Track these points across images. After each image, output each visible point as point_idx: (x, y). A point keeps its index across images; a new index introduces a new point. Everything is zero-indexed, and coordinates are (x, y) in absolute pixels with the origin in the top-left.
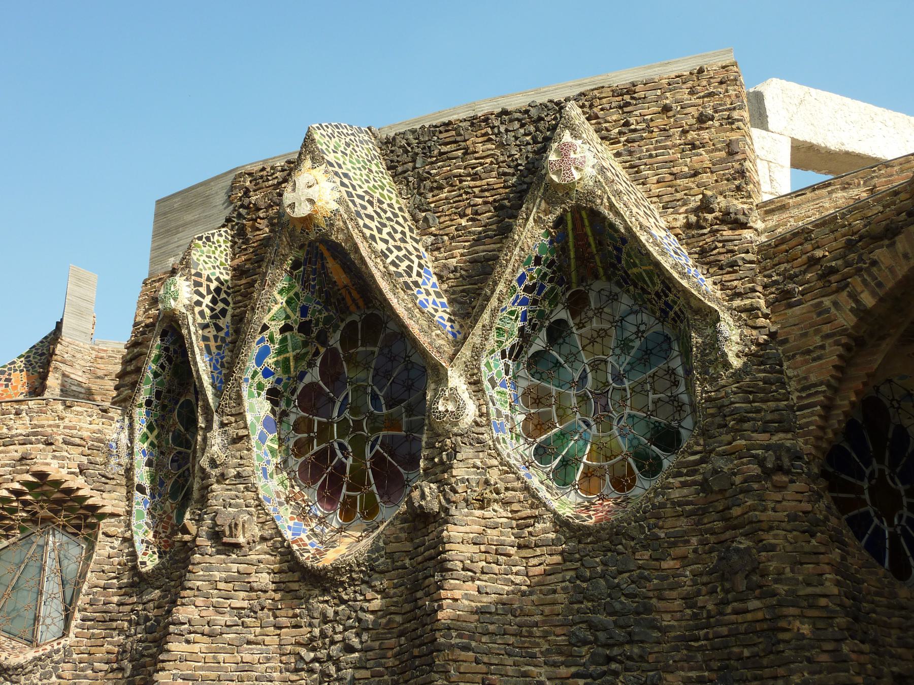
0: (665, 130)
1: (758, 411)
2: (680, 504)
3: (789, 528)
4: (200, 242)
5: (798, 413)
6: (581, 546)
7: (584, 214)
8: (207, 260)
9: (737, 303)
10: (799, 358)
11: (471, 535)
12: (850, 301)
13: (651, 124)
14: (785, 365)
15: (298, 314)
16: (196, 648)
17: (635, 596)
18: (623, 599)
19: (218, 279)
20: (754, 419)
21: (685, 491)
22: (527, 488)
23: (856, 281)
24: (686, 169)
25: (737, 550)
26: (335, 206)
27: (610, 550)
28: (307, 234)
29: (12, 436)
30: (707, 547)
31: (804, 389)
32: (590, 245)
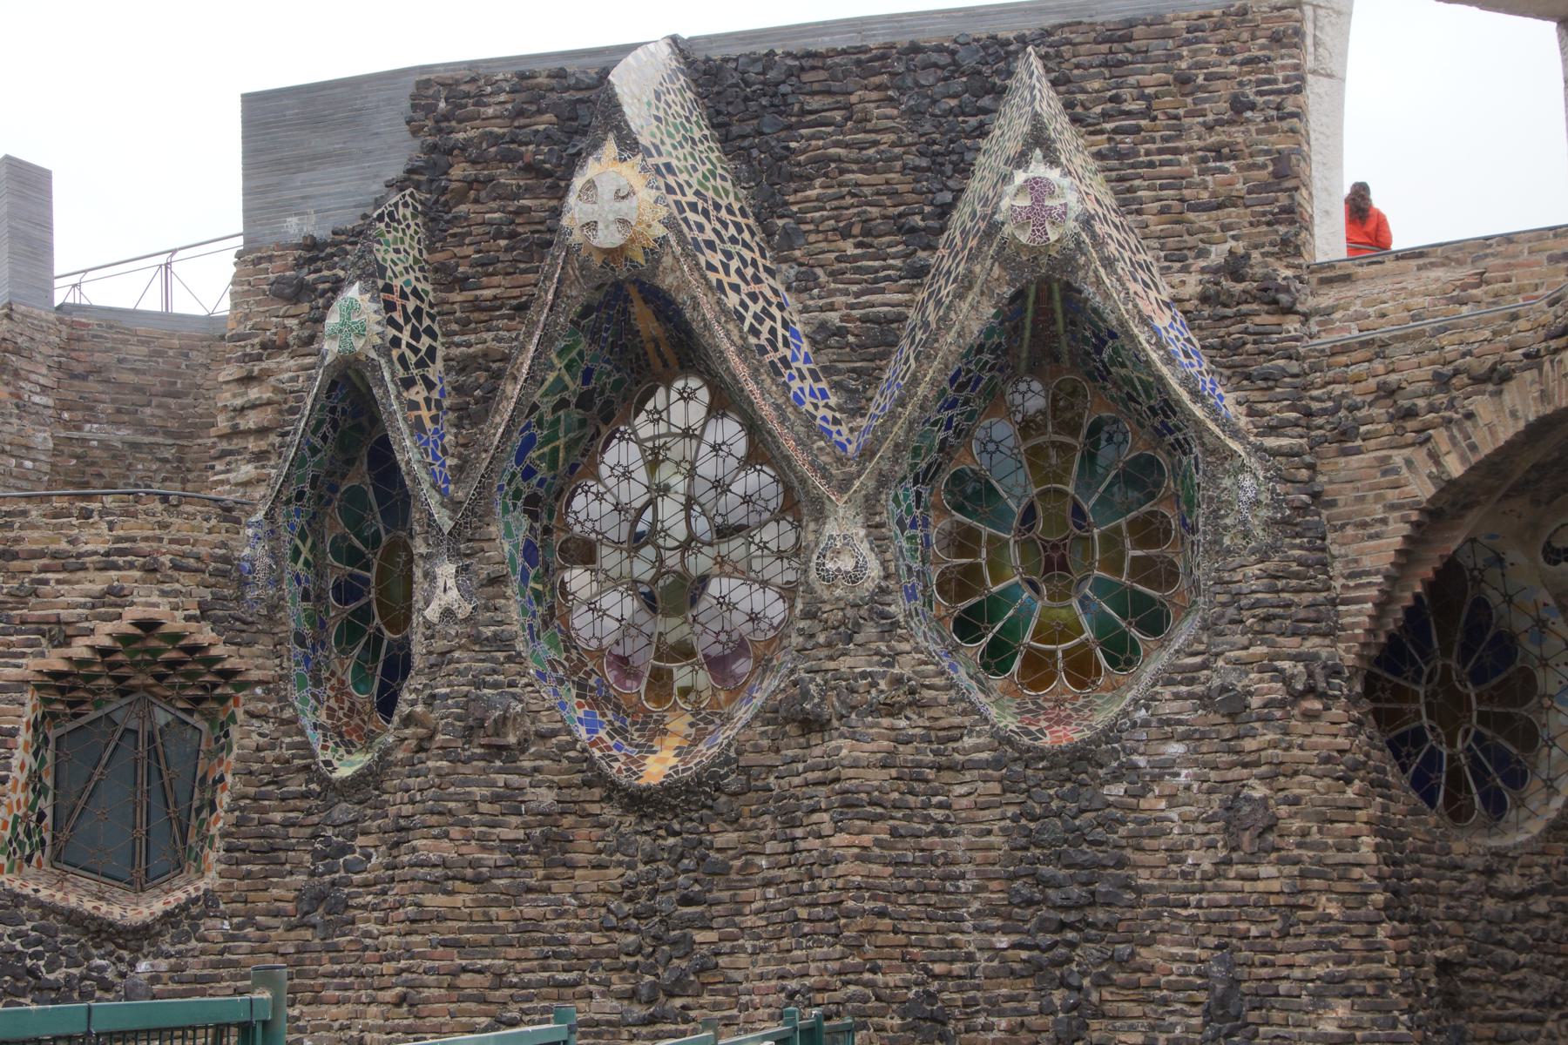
0: (1176, 117)
1: (1288, 605)
2: (1168, 722)
3: (1318, 773)
4: (382, 225)
5: (1341, 608)
6: (1029, 772)
7: (1056, 286)
8: (395, 257)
9: (1271, 442)
10: (1350, 531)
11: (879, 756)
12: (1430, 463)
13: (1155, 103)
14: (1330, 537)
15: (579, 381)
16: (458, 900)
17: (1101, 843)
18: (1084, 847)
19: (415, 292)
20: (1281, 617)
21: (1177, 705)
23: (1440, 436)
24: (1205, 195)
25: (1249, 799)
26: (659, 231)
27: (1069, 780)
28: (613, 269)
29: (79, 556)
30: (1205, 785)
31: (1352, 576)
32: (1054, 322)
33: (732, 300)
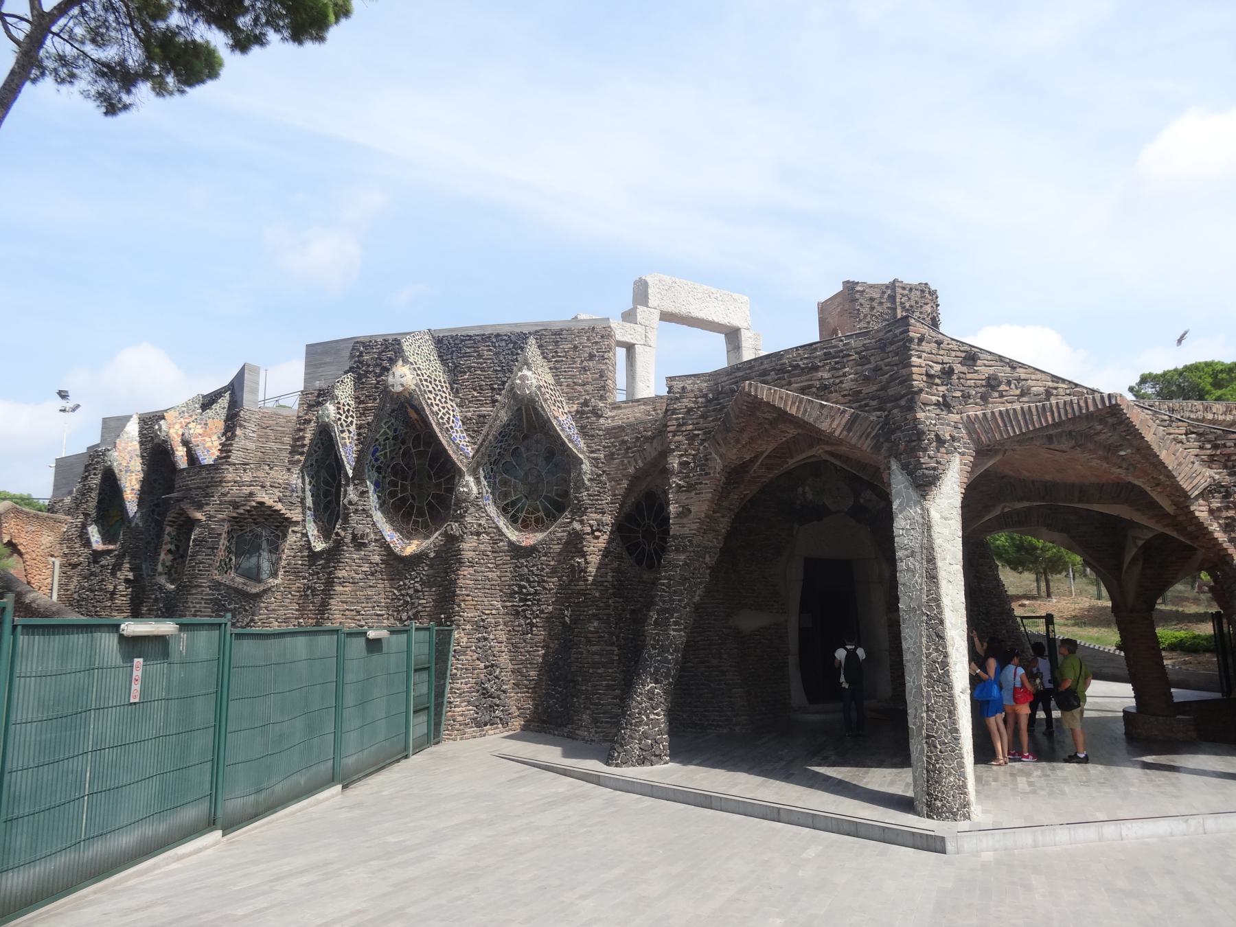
22: (497, 528)
26: (413, 387)
33: (435, 409)
